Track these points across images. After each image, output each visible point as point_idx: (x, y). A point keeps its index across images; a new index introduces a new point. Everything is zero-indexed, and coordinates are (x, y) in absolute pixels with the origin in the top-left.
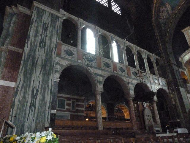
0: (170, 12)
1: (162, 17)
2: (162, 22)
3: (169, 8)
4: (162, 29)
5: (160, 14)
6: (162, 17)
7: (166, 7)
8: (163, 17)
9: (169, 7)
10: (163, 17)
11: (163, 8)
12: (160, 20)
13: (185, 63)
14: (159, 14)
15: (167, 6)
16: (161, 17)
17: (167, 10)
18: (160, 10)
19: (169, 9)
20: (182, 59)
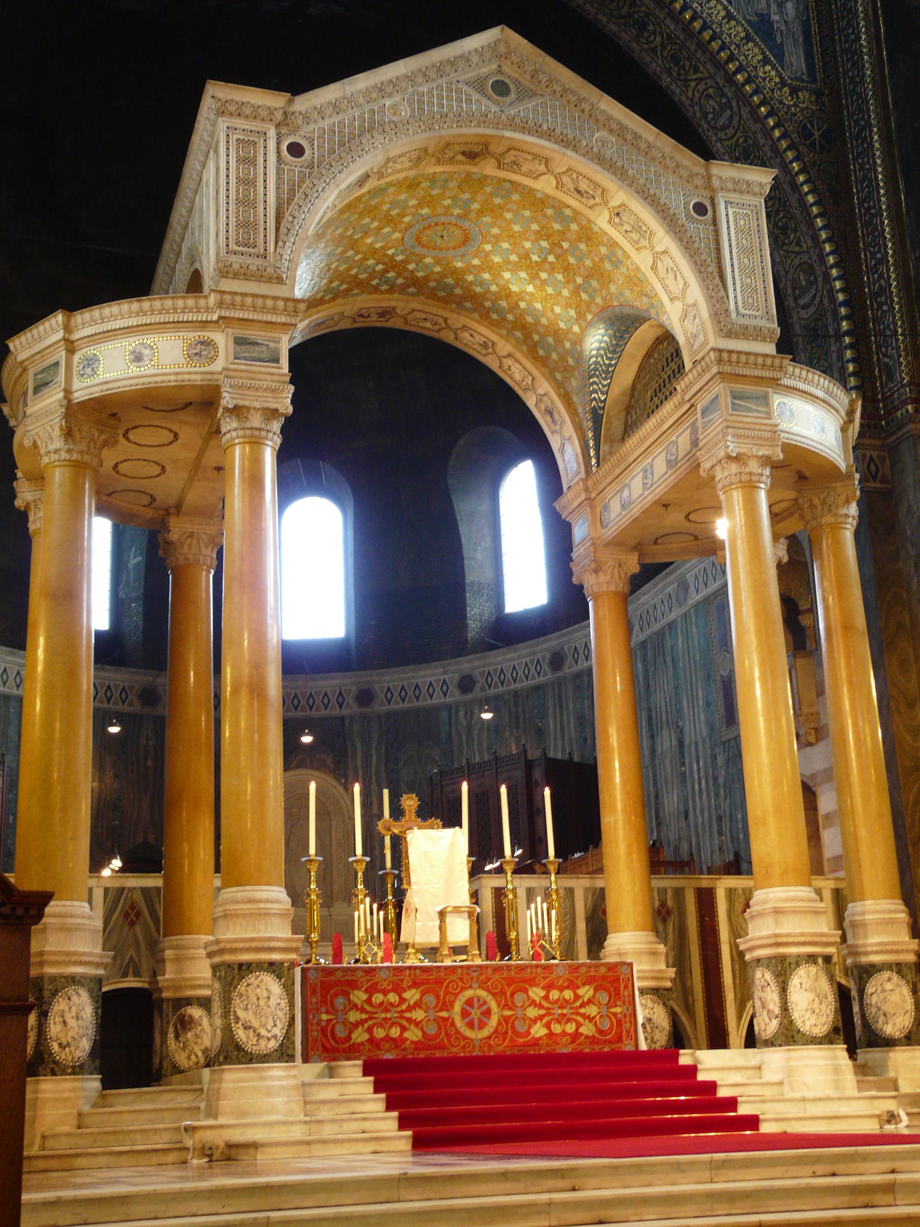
20: (71, 347)
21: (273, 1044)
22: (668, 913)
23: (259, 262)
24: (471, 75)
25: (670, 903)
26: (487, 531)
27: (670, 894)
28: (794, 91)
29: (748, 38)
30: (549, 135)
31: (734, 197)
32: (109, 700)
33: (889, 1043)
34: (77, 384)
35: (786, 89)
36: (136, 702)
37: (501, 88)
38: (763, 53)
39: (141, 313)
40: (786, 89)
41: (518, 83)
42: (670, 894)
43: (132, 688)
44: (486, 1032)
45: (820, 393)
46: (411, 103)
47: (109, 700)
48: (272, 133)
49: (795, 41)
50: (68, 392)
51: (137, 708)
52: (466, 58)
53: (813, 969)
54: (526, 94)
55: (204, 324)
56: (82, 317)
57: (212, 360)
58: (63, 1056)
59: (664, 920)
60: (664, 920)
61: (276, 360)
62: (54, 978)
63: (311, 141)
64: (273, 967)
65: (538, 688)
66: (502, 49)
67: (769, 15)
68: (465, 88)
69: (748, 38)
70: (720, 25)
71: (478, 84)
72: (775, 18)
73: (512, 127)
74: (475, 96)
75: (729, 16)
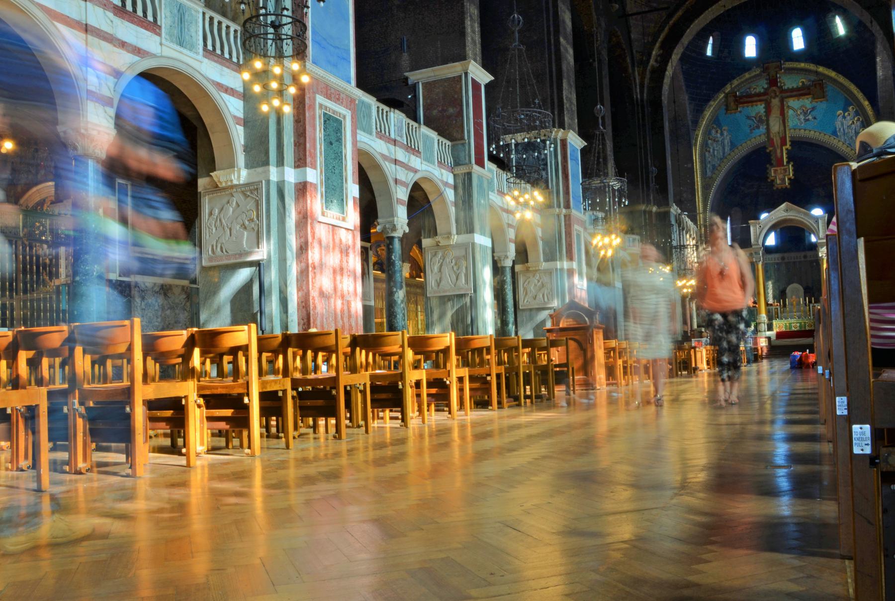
0: (726, 150)
1: (711, 151)
2: (709, 159)
3: (726, 141)
4: (706, 174)
5: (710, 142)
6: (711, 151)
7: (722, 134)
9: (728, 138)
10: (714, 150)
11: (717, 132)
12: (707, 153)
14: (707, 141)
15: (725, 133)
17: (723, 142)
18: (710, 133)
37: (787, 210)
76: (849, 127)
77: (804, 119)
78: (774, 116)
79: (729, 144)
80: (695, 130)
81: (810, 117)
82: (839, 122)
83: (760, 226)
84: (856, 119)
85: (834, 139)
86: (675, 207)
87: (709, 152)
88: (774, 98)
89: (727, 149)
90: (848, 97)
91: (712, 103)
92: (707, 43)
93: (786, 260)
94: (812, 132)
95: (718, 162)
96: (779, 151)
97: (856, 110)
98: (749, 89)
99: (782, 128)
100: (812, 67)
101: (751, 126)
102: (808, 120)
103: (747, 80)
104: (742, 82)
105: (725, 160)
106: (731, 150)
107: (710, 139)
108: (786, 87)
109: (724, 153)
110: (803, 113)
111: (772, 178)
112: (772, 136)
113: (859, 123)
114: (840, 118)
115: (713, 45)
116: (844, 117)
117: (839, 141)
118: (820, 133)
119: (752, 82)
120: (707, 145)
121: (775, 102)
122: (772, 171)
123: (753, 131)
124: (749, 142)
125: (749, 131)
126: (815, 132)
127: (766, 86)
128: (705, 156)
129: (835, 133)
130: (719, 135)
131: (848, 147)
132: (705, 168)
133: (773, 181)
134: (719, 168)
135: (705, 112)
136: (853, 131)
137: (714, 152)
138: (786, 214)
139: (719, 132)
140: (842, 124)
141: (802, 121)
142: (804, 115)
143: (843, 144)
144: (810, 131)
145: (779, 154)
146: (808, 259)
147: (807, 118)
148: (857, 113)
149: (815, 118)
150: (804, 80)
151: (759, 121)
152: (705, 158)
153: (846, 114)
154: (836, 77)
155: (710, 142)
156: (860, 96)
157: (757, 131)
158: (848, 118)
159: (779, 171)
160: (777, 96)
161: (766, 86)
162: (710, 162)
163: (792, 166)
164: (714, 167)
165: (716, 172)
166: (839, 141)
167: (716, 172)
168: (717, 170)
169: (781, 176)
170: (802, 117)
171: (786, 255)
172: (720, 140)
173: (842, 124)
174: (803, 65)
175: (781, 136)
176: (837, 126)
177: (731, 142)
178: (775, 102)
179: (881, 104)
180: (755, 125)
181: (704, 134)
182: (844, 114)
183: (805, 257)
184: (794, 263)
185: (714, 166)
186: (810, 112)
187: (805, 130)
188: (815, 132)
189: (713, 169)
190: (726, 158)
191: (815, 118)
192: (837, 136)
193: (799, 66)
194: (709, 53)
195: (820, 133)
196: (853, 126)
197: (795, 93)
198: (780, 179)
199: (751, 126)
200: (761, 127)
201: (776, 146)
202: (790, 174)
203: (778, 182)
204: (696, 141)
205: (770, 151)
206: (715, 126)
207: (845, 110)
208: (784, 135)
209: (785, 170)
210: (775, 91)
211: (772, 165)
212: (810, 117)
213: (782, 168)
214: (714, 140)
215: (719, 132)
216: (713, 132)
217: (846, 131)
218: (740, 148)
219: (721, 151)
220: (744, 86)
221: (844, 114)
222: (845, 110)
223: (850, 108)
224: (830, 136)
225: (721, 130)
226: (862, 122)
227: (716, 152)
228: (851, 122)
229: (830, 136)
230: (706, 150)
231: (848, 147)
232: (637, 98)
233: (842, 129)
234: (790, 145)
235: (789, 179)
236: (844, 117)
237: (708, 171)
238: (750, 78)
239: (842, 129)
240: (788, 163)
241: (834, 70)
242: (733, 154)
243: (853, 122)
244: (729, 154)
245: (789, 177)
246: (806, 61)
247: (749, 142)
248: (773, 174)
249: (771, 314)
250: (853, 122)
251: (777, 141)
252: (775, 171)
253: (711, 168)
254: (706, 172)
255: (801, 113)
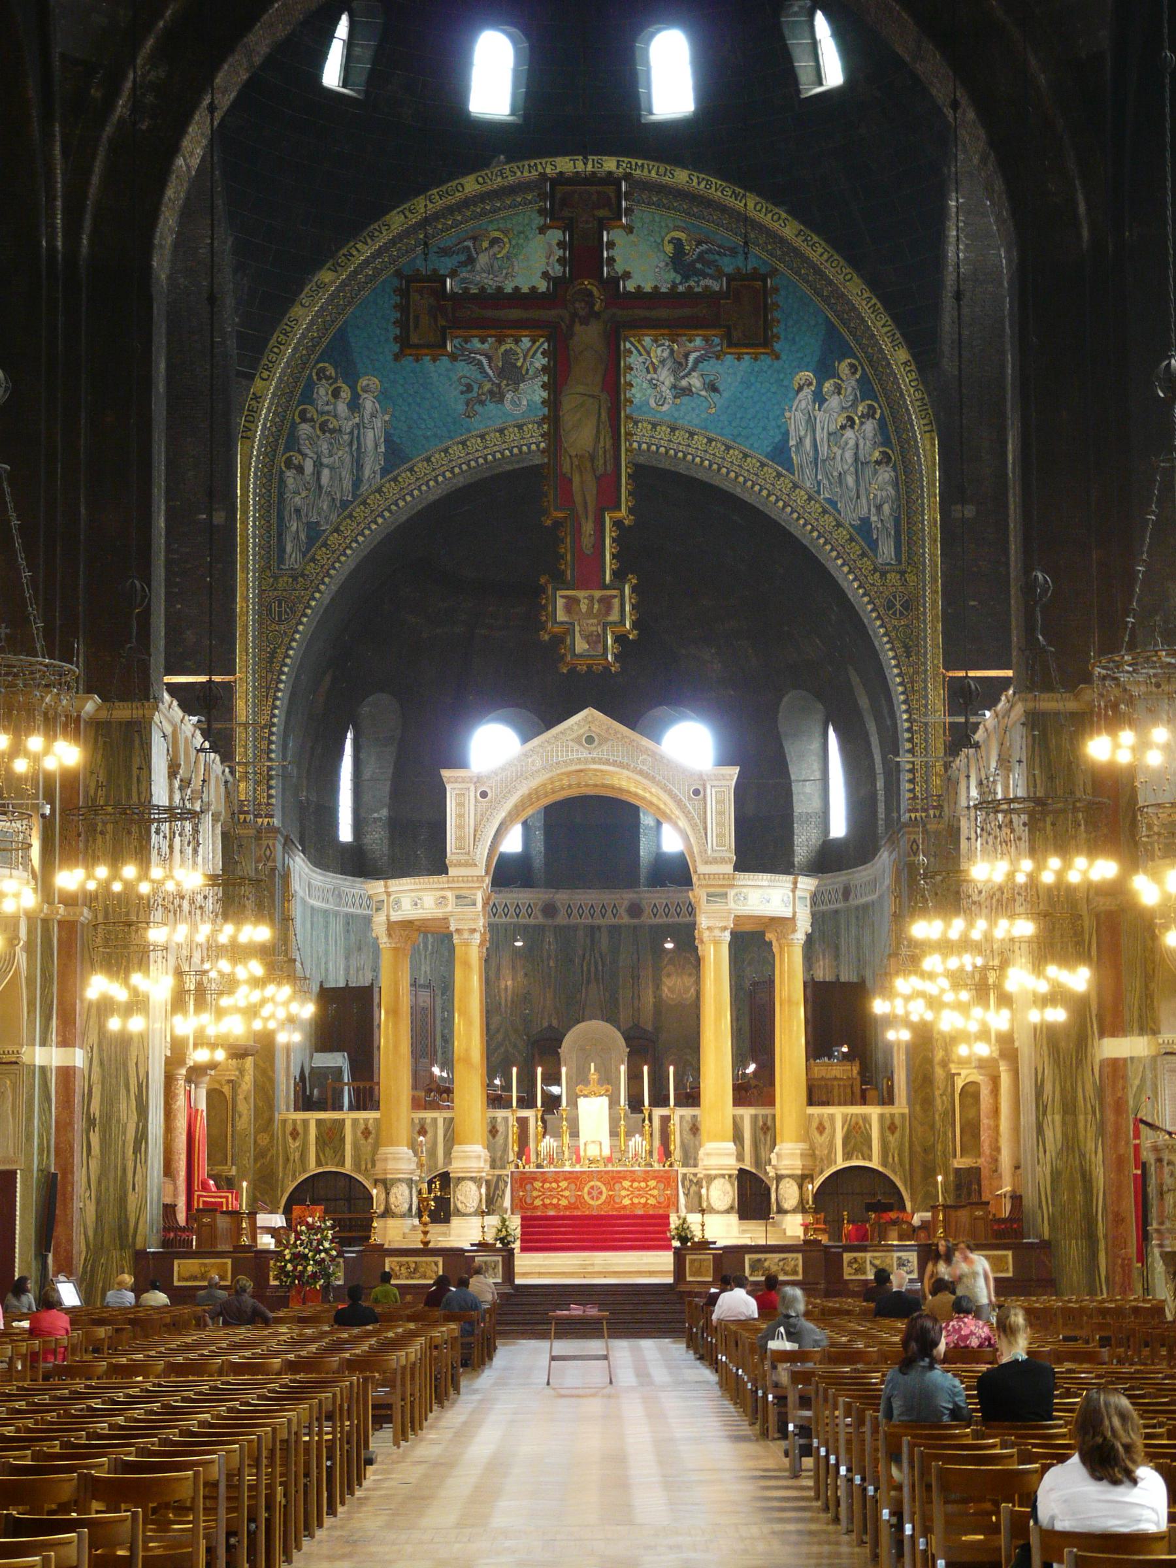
0: (367, 472)
1: (309, 466)
3: (370, 434)
4: (281, 560)
5: (305, 429)
6: (309, 466)
7: (355, 405)
8: (318, 465)
9: (378, 423)
10: (318, 465)
11: (336, 394)
13: (393, 919)
14: (294, 426)
15: (369, 404)
16: (305, 456)
17: (356, 438)
18: (307, 397)
19: (369, 438)
20: (388, 894)
21: (472, 1210)
22: (768, 1129)
23: (466, 857)
24: (574, 735)
25: (769, 1123)
26: (817, 766)
27: (769, 1118)
28: (883, 574)
29: (852, 539)
30: (614, 764)
31: (716, 783)
32: (518, 916)
33: (786, 1212)
34: (392, 913)
35: (878, 574)
36: (539, 914)
37: (590, 740)
38: (862, 548)
39: (415, 883)
40: (878, 574)
41: (599, 735)
42: (769, 1118)
43: (536, 905)
44: (599, 1202)
45: (765, 883)
46: (542, 758)
47: (518, 916)
48: (472, 789)
49: (888, 535)
50: (388, 916)
51: (541, 920)
52: (571, 729)
53: (722, 1180)
54: (603, 740)
55: (442, 889)
56: (391, 882)
57: (446, 905)
58: (396, 1210)
59: (765, 1133)
60: (765, 1133)
61: (474, 904)
62: (392, 1179)
63: (491, 788)
64: (472, 1179)
65: (836, 912)
66: (590, 719)
67: (869, 518)
68: (571, 743)
69: (852, 539)
70: (831, 533)
71: (577, 740)
72: (874, 518)
73: (594, 761)
74: (576, 747)
75: (839, 525)
76: (834, 436)
77: (674, 387)
78: (580, 389)
79: (382, 449)
80: (251, 377)
81: (695, 381)
82: (799, 414)
83: (484, 795)
84: (861, 408)
85: (779, 475)
86: (177, 713)
87: (300, 469)
88: (585, 321)
89: (371, 467)
90: (836, 322)
91: (326, 276)
92: (330, 36)
93: (561, 919)
94: (700, 441)
95: (333, 517)
96: (588, 528)
97: (864, 373)
98: (474, 239)
99: (606, 442)
100: (716, 189)
101: (469, 388)
102: (687, 391)
103: (466, 203)
104: (450, 210)
105: (359, 512)
106: (385, 471)
107: (304, 419)
108: (630, 286)
109: (357, 483)
110: (669, 363)
111: (557, 629)
112: (566, 468)
113: (870, 426)
114: (807, 392)
115: (350, 44)
116: (819, 398)
117: (795, 486)
118: (728, 448)
119: (484, 213)
120: (292, 443)
121: (588, 336)
122: (560, 602)
123: (477, 407)
124: (456, 451)
125: (461, 408)
126: (710, 440)
127: (557, 270)
128: (282, 482)
129: (781, 453)
130: (342, 408)
131: (825, 511)
132: (280, 535)
133: (558, 640)
134: (334, 539)
135: (296, 311)
136: (849, 455)
137: (318, 475)
138: (583, 754)
139: (346, 394)
140: (811, 423)
141: (666, 390)
142: (674, 372)
143: (810, 498)
144: (692, 434)
145: (587, 542)
146: (647, 919)
147: (684, 383)
148: (866, 389)
149: (713, 388)
150: (682, 236)
151: (501, 373)
152: (281, 494)
153: (828, 386)
154: (799, 243)
155: (305, 429)
156: (880, 326)
157: (491, 406)
158: (834, 402)
159: (584, 607)
160: (597, 315)
161: (557, 270)
162: (298, 511)
163: (634, 589)
164: (314, 533)
165: (321, 554)
166: (795, 486)
167: (321, 554)
168: (325, 545)
169: (593, 626)
170: (665, 376)
171: (562, 897)
172: (347, 426)
173: (811, 423)
174: (681, 177)
175: (601, 471)
176: (792, 433)
177: (387, 441)
178: (588, 336)
179: (949, 366)
180: (487, 386)
181: (285, 394)
182: (820, 385)
183: (635, 910)
184: (593, 930)
185: (314, 533)
186: (697, 361)
187: (673, 430)
188: (710, 440)
189: (311, 541)
190: (364, 503)
191: (713, 388)
192: (790, 469)
193: (667, 179)
194: (332, 76)
195: (728, 448)
196: (849, 433)
197: (663, 313)
198: (587, 638)
199: (469, 388)
200: (509, 396)
201: (580, 509)
202: (622, 622)
203: (581, 646)
204: (252, 420)
205: (557, 524)
206: (331, 371)
207: (825, 370)
208: (609, 468)
209: (606, 602)
210: (591, 294)
211: (560, 581)
212: (695, 381)
213: (598, 594)
214: (323, 427)
215: (346, 394)
216: (322, 392)
217: (824, 450)
218: (421, 467)
219: (346, 474)
220: (456, 224)
221: (820, 385)
222: (825, 370)
223: (844, 367)
224: (763, 465)
225: (353, 388)
226: (882, 425)
227: (326, 472)
228: (842, 420)
229: (763, 465)
230: (289, 464)
231: (825, 511)
232: (52, 248)
233: (808, 442)
234: (631, 511)
235: (620, 639)
236: (819, 398)
237: (289, 548)
238: (483, 197)
239: (808, 442)
240: (620, 576)
241: (796, 212)
242: (391, 490)
243: (850, 419)
244: (379, 491)
245: (620, 630)
246: (696, 163)
247: (456, 451)
248: (561, 616)
249: (500, 1139)
250: (850, 419)
251: (584, 488)
252: (572, 603)
253: (303, 536)
254: (282, 550)
255: (662, 362)
